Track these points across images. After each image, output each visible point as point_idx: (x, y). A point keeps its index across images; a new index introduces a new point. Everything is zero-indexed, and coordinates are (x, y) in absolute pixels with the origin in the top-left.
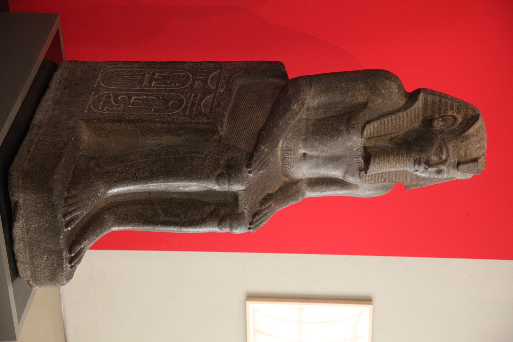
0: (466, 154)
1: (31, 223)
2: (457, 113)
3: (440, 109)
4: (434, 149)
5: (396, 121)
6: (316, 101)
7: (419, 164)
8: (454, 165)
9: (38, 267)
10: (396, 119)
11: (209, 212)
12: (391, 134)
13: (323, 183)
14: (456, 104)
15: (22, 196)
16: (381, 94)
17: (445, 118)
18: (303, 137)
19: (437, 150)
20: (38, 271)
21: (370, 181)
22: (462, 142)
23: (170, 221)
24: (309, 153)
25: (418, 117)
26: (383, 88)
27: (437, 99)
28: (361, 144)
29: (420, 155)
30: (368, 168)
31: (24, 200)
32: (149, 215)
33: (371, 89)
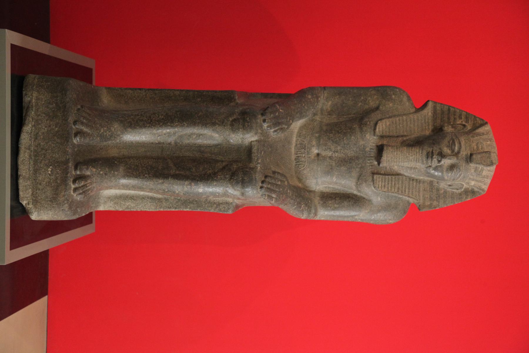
0: (478, 148)
1: (40, 126)
2: (466, 122)
3: (449, 119)
4: (446, 141)
5: (407, 123)
6: (330, 103)
7: (432, 157)
8: (467, 159)
9: (40, 184)
10: (406, 120)
11: (221, 167)
12: (402, 136)
13: (336, 197)
14: (464, 113)
15: (35, 94)
16: (392, 99)
18: (317, 135)
19: (449, 142)
20: (39, 190)
21: (383, 188)
22: (473, 137)
23: (181, 174)
24: (324, 153)
25: (428, 125)
26: (394, 94)
27: (446, 108)
28: (374, 143)
29: (433, 147)
30: (381, 156)
31: (37, 99)
32: (160, 168)
33: (382, 94)
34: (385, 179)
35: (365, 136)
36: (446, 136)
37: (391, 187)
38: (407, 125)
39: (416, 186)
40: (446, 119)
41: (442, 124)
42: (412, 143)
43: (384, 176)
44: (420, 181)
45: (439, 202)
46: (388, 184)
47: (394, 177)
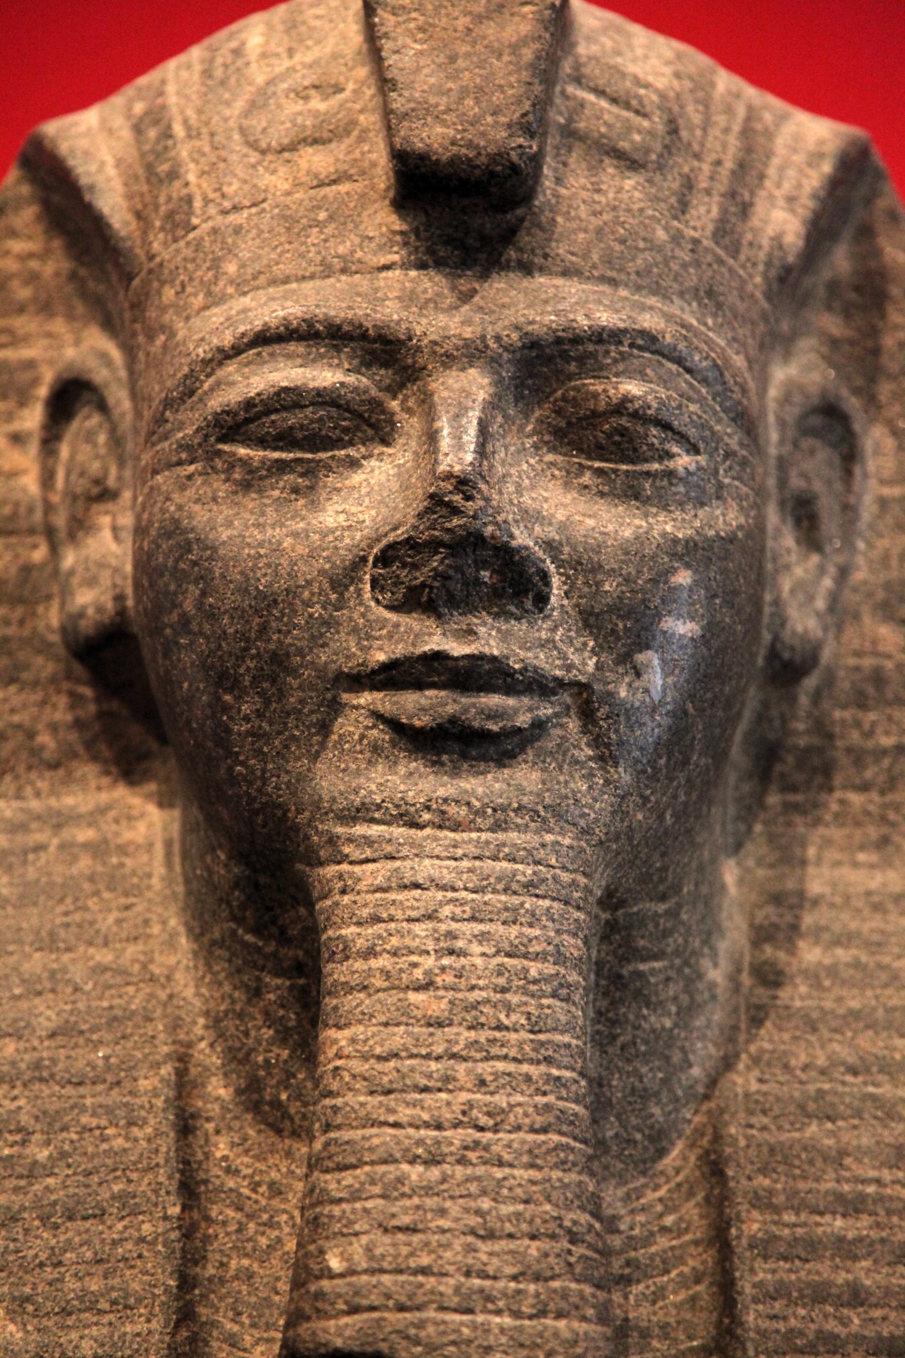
12: (186, 1126)
17: (60, 520)
19: (251, 481)
22: (178, 222)
25: (59, 821)
36: (174, 529)
39: (845, 939)
41: (44, 667)
42: (276, 986)
44: (777, 899)
47: (753, 1225)
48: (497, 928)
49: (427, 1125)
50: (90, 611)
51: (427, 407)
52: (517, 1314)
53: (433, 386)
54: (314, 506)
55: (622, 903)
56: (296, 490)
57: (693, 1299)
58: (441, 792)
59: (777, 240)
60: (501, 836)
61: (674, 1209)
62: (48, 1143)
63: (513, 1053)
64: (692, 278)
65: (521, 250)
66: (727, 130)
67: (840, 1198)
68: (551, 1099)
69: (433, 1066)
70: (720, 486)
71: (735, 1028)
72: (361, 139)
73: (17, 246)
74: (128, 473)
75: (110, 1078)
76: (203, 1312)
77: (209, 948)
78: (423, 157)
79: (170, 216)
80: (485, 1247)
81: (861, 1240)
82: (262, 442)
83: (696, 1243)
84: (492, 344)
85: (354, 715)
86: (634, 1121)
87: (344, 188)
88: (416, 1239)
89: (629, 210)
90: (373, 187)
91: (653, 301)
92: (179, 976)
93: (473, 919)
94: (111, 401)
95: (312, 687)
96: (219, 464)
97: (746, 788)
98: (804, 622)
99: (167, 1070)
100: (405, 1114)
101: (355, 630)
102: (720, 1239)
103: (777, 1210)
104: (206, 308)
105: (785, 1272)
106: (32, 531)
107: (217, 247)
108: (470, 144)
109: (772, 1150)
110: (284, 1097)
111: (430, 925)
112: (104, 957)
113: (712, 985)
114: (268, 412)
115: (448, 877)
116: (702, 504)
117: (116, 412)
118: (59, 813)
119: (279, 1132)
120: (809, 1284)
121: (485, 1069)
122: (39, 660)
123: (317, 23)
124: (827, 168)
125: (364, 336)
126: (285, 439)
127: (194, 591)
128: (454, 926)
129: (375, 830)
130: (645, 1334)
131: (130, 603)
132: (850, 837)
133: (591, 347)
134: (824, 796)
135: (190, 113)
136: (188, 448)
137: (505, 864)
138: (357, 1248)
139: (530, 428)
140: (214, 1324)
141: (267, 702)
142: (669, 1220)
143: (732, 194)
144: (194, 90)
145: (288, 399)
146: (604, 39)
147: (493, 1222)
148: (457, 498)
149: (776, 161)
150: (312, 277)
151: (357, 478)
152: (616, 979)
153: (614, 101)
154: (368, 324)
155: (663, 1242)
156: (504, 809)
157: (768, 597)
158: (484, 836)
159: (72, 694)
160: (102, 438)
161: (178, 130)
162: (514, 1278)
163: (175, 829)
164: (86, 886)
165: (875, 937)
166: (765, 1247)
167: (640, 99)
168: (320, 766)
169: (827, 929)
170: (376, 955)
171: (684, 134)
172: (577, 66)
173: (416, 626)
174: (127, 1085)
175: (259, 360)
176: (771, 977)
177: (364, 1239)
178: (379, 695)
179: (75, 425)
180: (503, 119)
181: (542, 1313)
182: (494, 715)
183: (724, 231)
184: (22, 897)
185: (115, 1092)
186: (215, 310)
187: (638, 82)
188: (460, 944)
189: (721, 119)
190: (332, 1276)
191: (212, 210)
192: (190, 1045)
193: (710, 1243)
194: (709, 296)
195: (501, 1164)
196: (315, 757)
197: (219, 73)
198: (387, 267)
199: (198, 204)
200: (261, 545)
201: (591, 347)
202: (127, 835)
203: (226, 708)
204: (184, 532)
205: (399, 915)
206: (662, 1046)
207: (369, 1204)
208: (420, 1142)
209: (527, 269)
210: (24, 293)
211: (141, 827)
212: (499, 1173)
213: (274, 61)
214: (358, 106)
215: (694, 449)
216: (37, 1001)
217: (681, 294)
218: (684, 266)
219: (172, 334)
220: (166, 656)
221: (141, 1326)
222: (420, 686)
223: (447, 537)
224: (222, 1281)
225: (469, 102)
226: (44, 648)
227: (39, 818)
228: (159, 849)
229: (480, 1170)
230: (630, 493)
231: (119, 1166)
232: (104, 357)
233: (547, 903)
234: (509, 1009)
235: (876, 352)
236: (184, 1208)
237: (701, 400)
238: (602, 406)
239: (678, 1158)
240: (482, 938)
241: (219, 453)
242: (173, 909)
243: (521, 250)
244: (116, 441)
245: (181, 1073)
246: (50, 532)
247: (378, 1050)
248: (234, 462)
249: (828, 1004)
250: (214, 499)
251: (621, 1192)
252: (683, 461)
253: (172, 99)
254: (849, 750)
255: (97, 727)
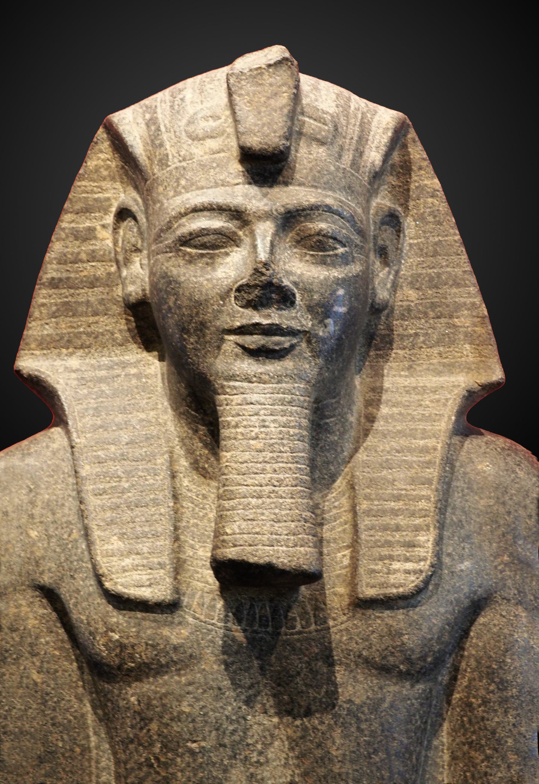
17: (121, 258)
19: (191, 260)
22: (163, 162)
25: (124, 365)
34: (377, 544)
35: (175, 649)
36: (165, 275)
37: (413, 514)
38: (124, 457)
40: (92, 296)
41: (117, 309)
43: (363, 550)
44: (373, 390)
45: (458, 307)
46: (398, 528)
47: (364, 505)
48: (279, 418)
49: (257, 485)
50: (134, 294)
51: (252, 233)
52: (288, 546)
53: (254, 228)
54: (214, 269)
55: (321, 401)
56: (207, 264)
57: (344, 530)
58: (260, 371)
59: (373, 163)
60: (280, 385)
61: (338, 500)
62: (127, 481)
63: (285, 460)
64: (343, 183)
65: (284, 177)
66: (355, 125)
67: (393, 495)
68: (298, 475)
69: (259, 465)
70: (353, 257)
71: (359, 437)
72: (228, 137)
73: (102, 156)
74: (145, 244)
75: (147, 459)
76: (182, 537)
77: (180, 414)
78: (250, 149)
79: (160, 160)
80: (277, 525)
81: (399, 509)
82: (195, 247)
83: (345, 511)
84: (275, 213)
85: (229, 343)
86: (325, 471)
87: (222, 155)
88: (254, 523)
89: (321, 160)
90: (232, 155)
91: (330, 193)
92: (169, 423)
93: (271, 415)
94: (138, 218)
95: (214, 333)
96: (180, 254)
97: (363, 350)
98: (383, 294)
99: (166, 456)
100: (250, 481)
101: (229, 314)
102: (353, 510)
103: (372, 500)
104: (174, 196)
105: (375, 521)
106: (111, 261)
107: (178, 174)
108: (266, 144)
109: (371, 481)
110: (206, 466)
111: (256, 417)
112: (142, 416)
113: (352, 422)
114: (198, 236)
115: (263, 400)
116: (347, 264)
117: (140, 222)
118: (124, 362)
119: (205, 477)
120: (382, 525)
121: (276, 466)
122: (115, 307)
123: (211, 91)
124: (390, 134)
125: (230, 210)
126: (204, 246)
127: (173, 298)
128: (265, 417)
129: (237, 384)
130: (328, 542)
131: (147, 292)
132: (398, 366)
133: (309, 212)
134: (390, 351)
135: (167, 122)
136: (170, 247)
137: (281, 395)
138: (235, 527)
139: (288, 240)
140: (186, 541)
141: (199, 338)
142: (336, 504)
143: (357, 150)
144: (168, 112)
145: (204, 232)
146: (311, 95)
147: (279, 517)
148: (264, 270)
149: (372, 133)
150: (211, 187)
151: (228, 259)
152: (319, 426)
153: (315, 120)
154: (231, 205)
155: (334, 511)
156: (281, 376)
157: (370, 287)
158: (274, 385)
159: (126, 319)
160: (135, 230)
161: (163, 128)
162: (287, 535)
163: (165, 369)
164: (135, 390)
165: (407, 404)
166: (368, 513)
167: (324, 119)
168: (218, 361)
169: (390, 401)
170: (239, 427)
171: (340, 130)
172: (302, 108)
173: (250, 313)
174: (153, 461)
175: (194, 218)
176: (371, 419)
177: (238, 523)
178: (237, 337)
179: (125, 223)
180: (277, 135)
181: (296, 546)
182: (277, 344)
183: (355, 164)
184: (114, 394)
185: (149, 464)
186: (177, 198)
187: (324, 112)
188: (267, 424)
189: (352, 121)
190: (227, 534)
191: (176, 160)
192: (173, 447)
193: (350, 511)
194: (349, 189)
195: (282, 497)
196: (216, 358)
197: (176, 107)
198: (237, 184)
199: (170, 157)
200: (196, 283)
201: (309, 212)
202: (148, 371)
203: (185, 340)
204: (169, 277)
205: (246, 413)
206: (334, 446)
207: (239, 512)
208: (255, 491)
209: (286, 184)
210: (105, 173)
211: (153, 367)
212: (281, 501)
213: (196, 105)
214: (226, 125)
215: (344, 246)
216: (121, 432)
217: (339, 190)
218: (340, 179)
219: (162, 204)
220: (163, 319)
221: (162, 543)
222: (251, 334)
223: (260, 284)
224: (188, 527)
225: (266, 128)
226: (116, 303)
227: (117, 364)
228: (159, 376)
229: (275, 500)
230: (323, 262)
231: (152, 489)
232: (135, 200)
233: (295, 408)
234: (284, 445)
235: (408, 190)
236: (175, 503)
237: (347, 228)
238: (313, 233)
239: (340, 483)
240: (274, 421)
241: (180, 250)
242: (166, 399)
243: (284, 177)
244: (140, 233)
245: (171, 457)
246: (117, 262)
247: (240, 460)
248: (185, 254)
249: (390, 428)
250: (179, 266)
251: (320, 495)
252: (341, 250)
253: (160, 116)
254: (398, 335)
255: (136, 331)
